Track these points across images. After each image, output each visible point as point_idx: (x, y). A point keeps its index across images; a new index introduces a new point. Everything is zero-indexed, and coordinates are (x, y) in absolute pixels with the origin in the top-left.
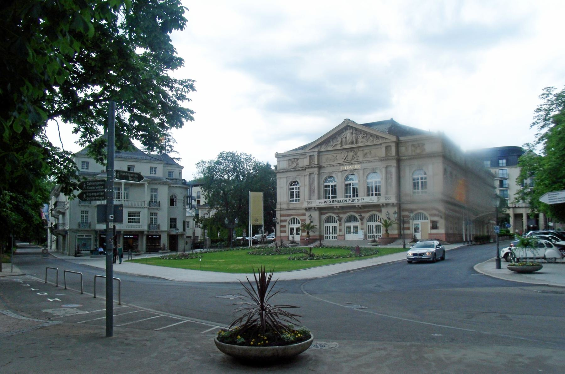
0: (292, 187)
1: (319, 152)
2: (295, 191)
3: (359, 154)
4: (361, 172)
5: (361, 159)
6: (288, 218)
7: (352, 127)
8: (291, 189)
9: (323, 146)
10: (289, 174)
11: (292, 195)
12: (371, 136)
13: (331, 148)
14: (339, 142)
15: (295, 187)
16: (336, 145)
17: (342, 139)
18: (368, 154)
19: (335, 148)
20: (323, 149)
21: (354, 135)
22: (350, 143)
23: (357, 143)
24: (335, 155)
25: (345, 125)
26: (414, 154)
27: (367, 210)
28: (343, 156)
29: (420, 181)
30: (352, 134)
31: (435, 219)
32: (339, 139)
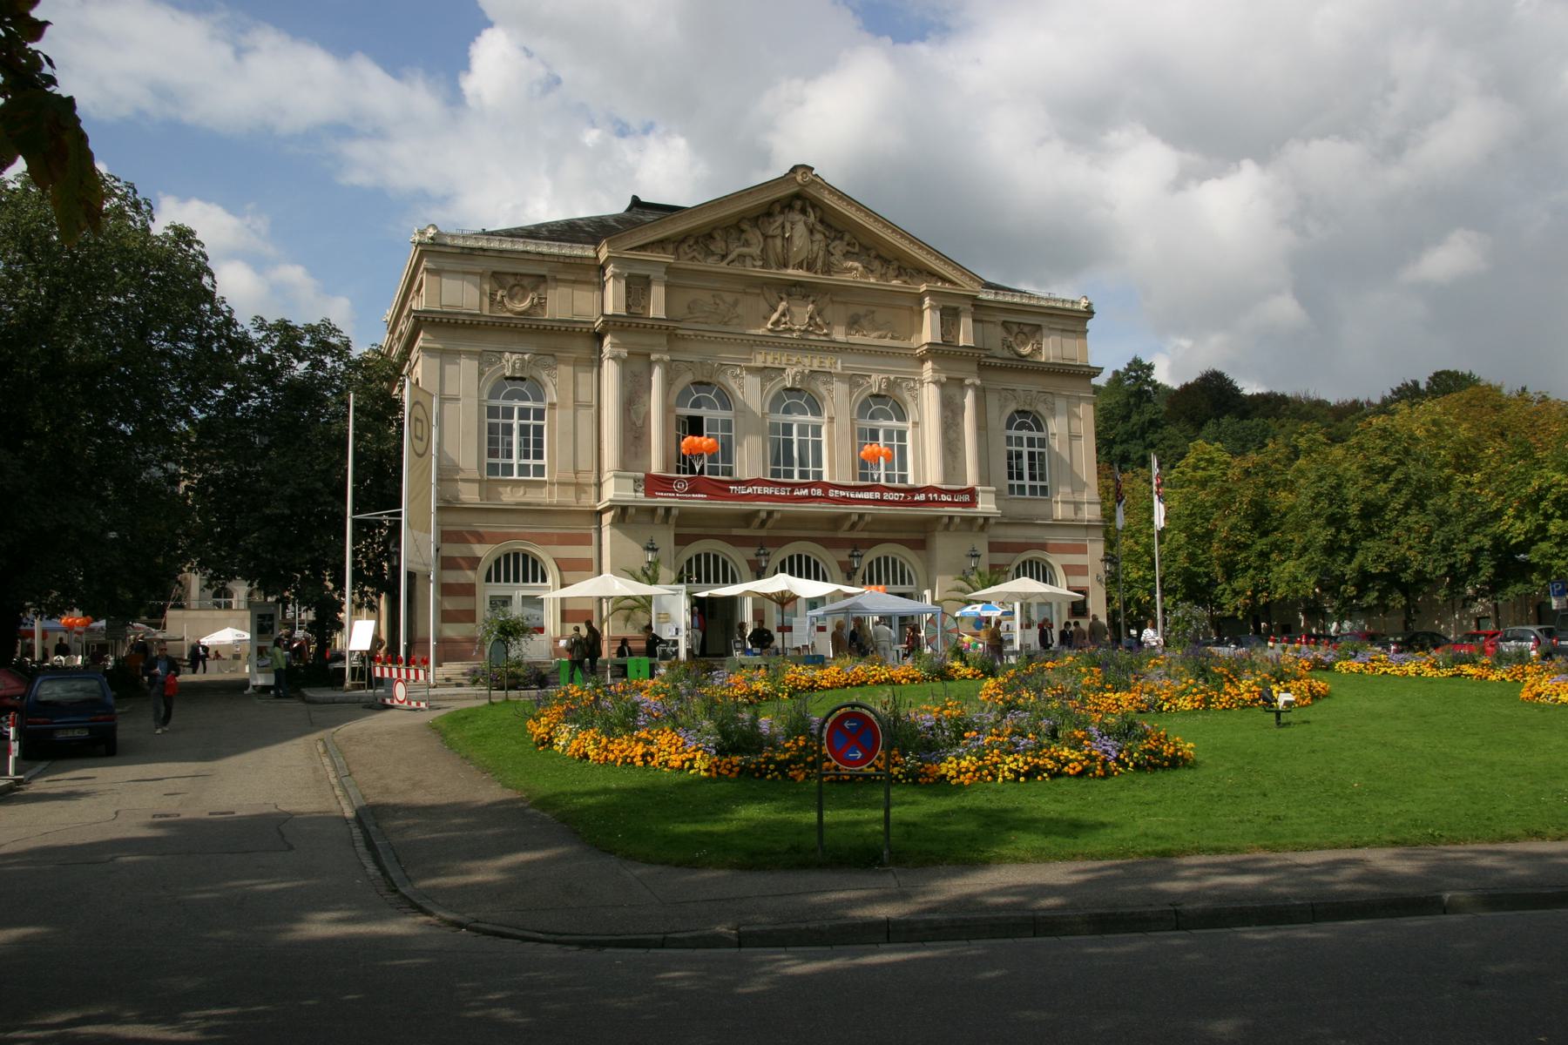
0: (501, 403)
1: (670, 269)
2: (516, 422)
3: (828, 312)
4: (840, 389)
5: (839, 335)
6: (484, 551)
7: (816, 205)
8: (493, 412)
9: (685, 247)
10: (490, 343)
11: (495, 441)
12: (878, 257)
13: (723, 267)
14: (755, 250)
15: (517, 404)
16: (742, 257)
17: (766, 237)
18: (864, 322)
19: (736, 269)
20: (685, 264)
21: (818, 236)
22: (800, 266)
23: (828, 269)
24: (729, 298)
25: (794, 189)
26: (1006, 354)
27: (865, 535)
28: (764, 306)
29: (1025, 450)
30: (811, 232)
31: (1080, 581)
32: (755, 236)
